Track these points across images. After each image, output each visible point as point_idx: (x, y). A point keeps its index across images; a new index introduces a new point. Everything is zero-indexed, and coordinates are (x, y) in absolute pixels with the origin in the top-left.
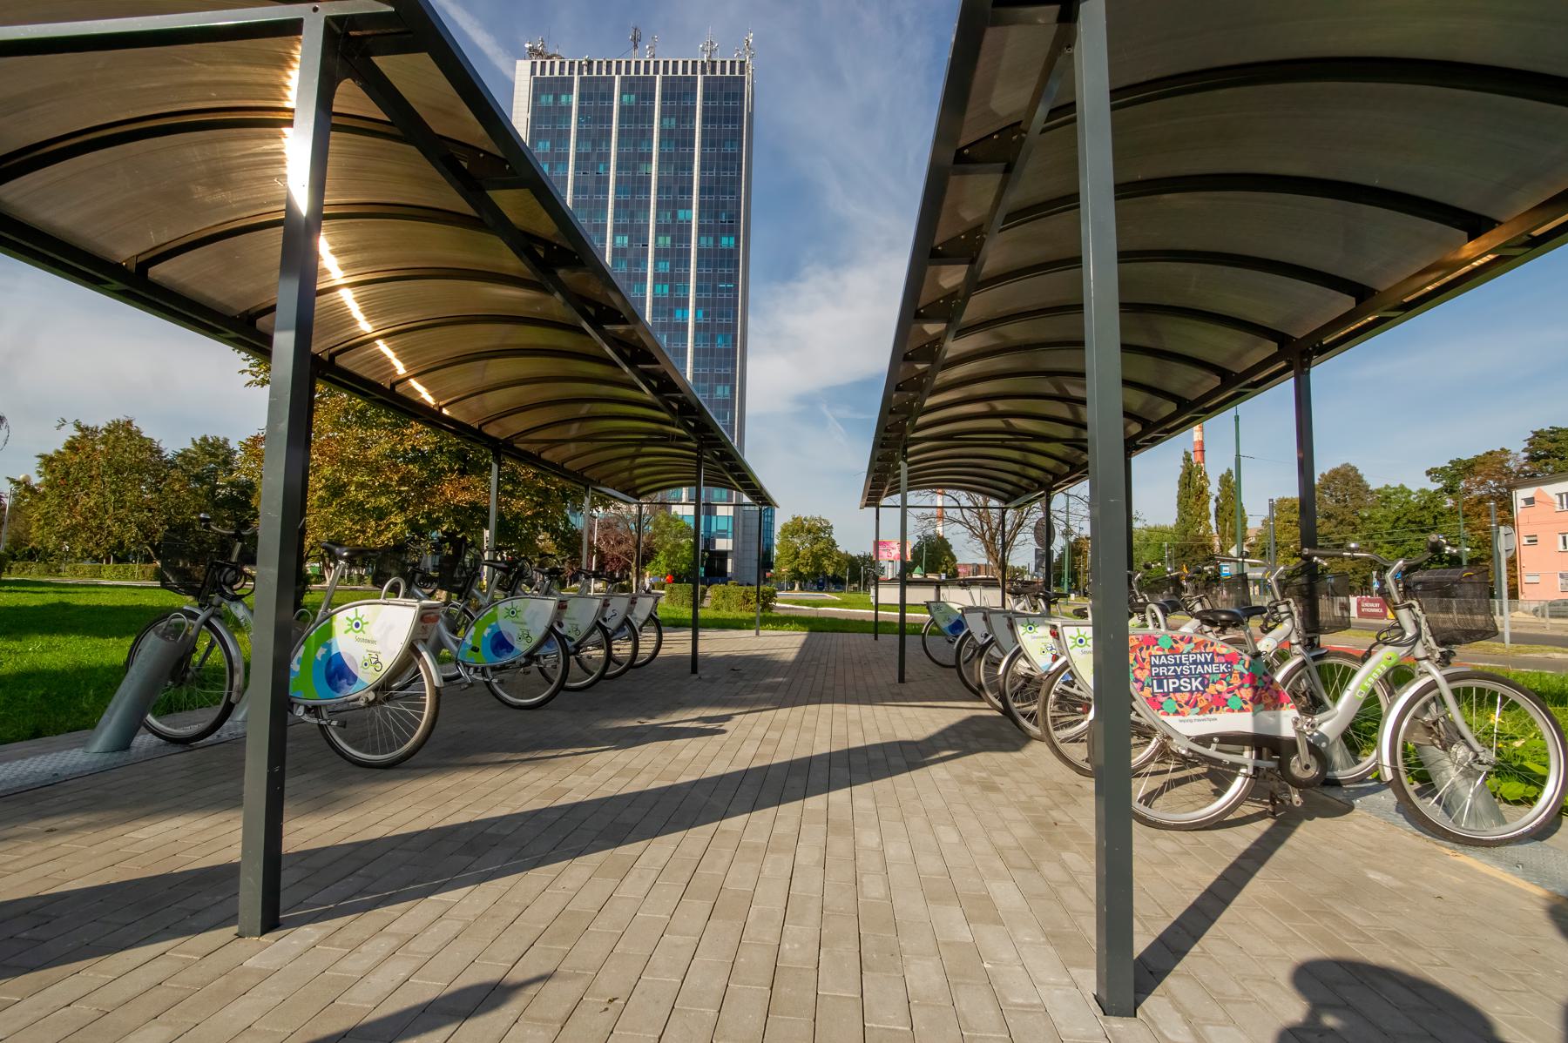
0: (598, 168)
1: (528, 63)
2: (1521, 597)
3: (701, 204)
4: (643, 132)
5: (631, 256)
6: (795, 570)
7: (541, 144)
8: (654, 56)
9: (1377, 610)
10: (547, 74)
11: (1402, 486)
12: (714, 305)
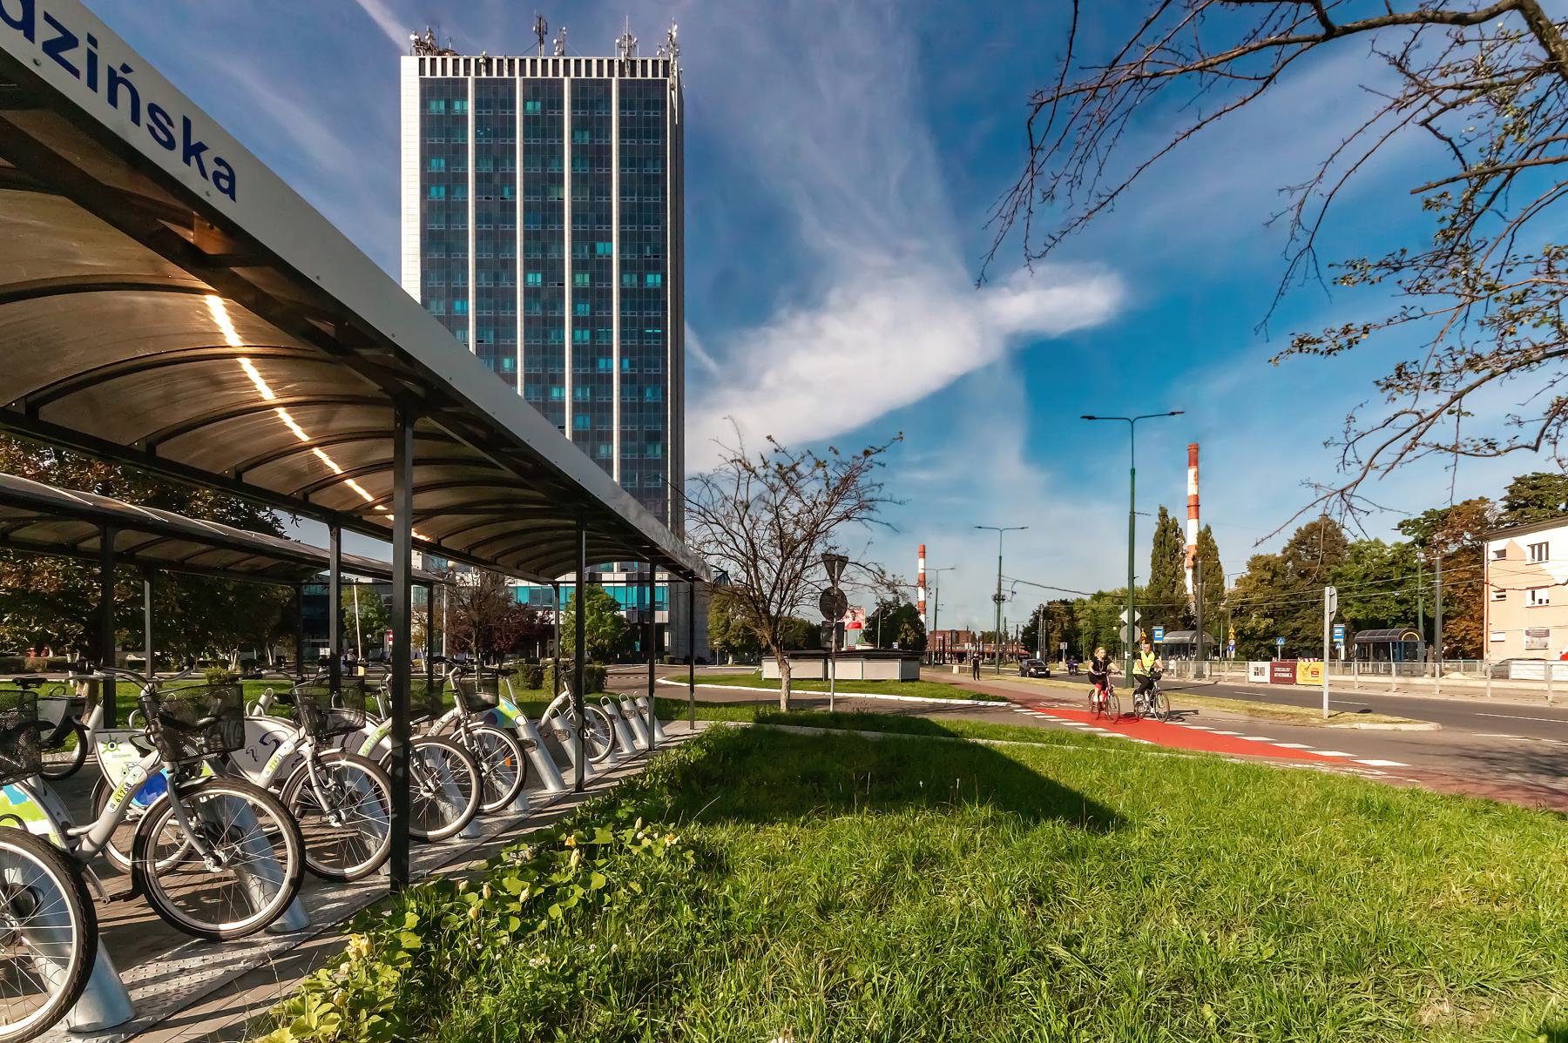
0: (502, 192)
1: (416, 60)
2: (1486, 656)
3: (622, 235)
4: (552, 147)
5: (545, 296)
6: (726, 643)
7: (434, 161)
8: (563, 54)
9: (1287, 675)
10: (439, 75)
11: (1377, 541)
12: (640, 354)
